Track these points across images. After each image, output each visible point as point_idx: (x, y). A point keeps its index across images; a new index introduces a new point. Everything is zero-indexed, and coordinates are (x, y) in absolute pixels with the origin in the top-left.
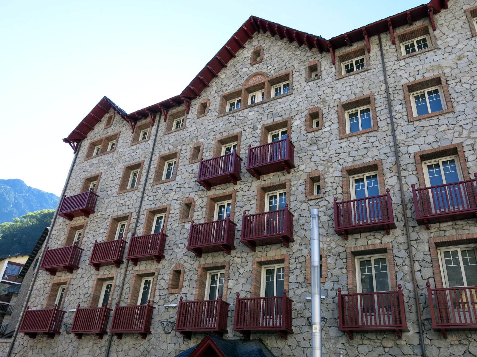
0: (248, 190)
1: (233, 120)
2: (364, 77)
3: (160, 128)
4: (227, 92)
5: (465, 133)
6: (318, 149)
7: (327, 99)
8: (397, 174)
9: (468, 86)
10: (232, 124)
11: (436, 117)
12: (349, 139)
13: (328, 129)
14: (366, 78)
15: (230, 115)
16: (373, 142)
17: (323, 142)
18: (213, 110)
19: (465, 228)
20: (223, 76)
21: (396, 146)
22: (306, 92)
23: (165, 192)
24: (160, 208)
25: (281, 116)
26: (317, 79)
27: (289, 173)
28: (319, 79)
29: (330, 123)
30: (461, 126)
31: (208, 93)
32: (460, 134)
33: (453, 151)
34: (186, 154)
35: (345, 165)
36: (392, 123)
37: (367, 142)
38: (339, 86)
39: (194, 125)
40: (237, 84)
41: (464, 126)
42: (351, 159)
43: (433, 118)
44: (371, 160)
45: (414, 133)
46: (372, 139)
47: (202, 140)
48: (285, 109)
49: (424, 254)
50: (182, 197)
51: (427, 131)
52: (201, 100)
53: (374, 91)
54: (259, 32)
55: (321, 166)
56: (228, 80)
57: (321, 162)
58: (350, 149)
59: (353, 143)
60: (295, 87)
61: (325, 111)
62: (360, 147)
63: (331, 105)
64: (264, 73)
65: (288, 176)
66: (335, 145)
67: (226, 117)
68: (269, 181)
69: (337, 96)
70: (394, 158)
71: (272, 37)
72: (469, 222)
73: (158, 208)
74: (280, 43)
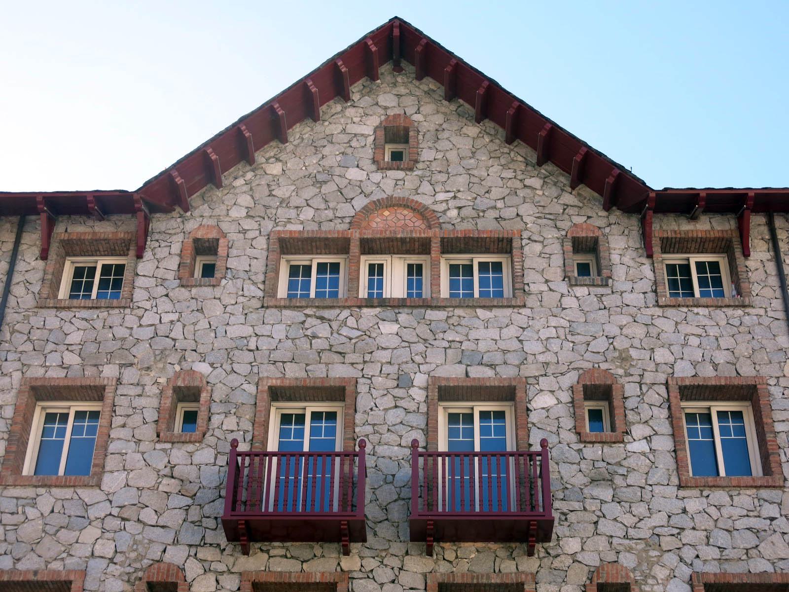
0: (393, 582)
1: (323, 330)
2: (736, 322)
3: (17, 278)
4: (290, 227)
6: (615, 499)
7: (633, 353)
10: (318, 344)
12: (705, 493)
13: (643, 446)
14: (741, 329)
15: (308, 311)
16: (772, 519)
17: (630, 481)
18: (242, 275)
20: (275, 169)
22: (569, 315)
23: (57, 520)
24: (39, 578)
25: (492, 366)
26: (602, 286)
27: (530, 554)
28: (607, 285)
29: (648, 431)
31: (220, 210)
34: (140, 400)
35: (699, 566)
37: (756, 513)
38: (666, 326)
39: (164, 305)
40: (330, 214)
42: (714, 553)
44: (769, 568)
46: (771, 510)
47: (203, 368)
48: (502, 345)
50: (133, 555)
52: (191, 225)
53: (765, 371)
54: (398, 69)
55: (627, 554)
56: (294, 187)
57: (627, 541)
58: (712, 523)
59: (719, 508)
60: (533, 288)
61: (631, 389)
62: (740, 524)
63: (649, 378)
64: (426, 208)
65: (529, 565)
66: (667, 498)
67: (298, 316)
68: (463, 567)
69: (662, 355)
71: (445, 103)
73: (31, 577)
74: (473, 130)
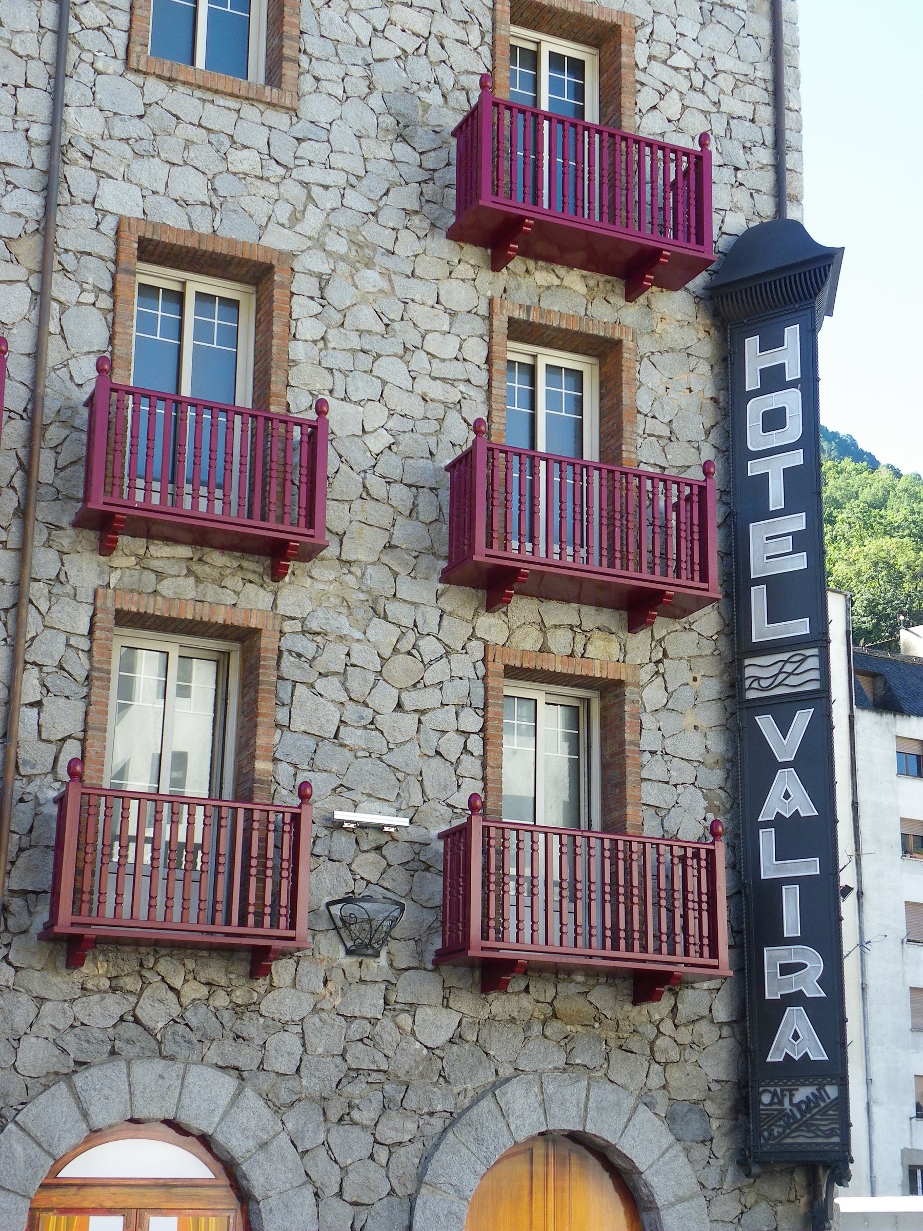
5: (313, 220)
8: (34, 281)
9: (365, 34)
11: (233, 104)
19: (228, 582)
21: (56, 149)
30: (305, 185)
32: (296, 218)
33: (258, 274)
36: (61, 34)
41: (316, 191)
43: (220, 101)
45: (136, 129)
49: (68, 645)
51: (188, 144)
70: (36, 202)
72: (245, 564)
